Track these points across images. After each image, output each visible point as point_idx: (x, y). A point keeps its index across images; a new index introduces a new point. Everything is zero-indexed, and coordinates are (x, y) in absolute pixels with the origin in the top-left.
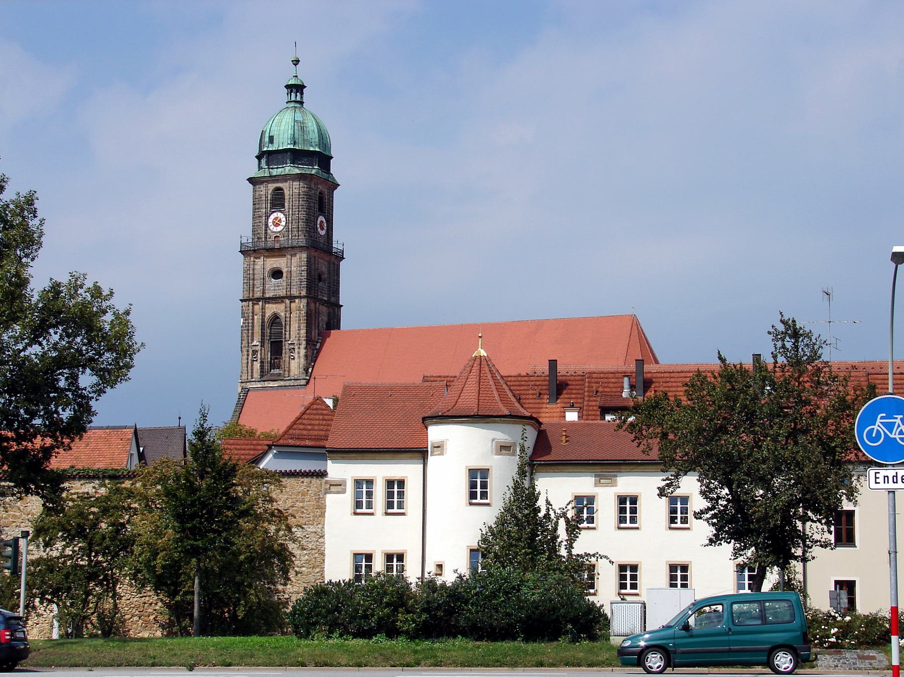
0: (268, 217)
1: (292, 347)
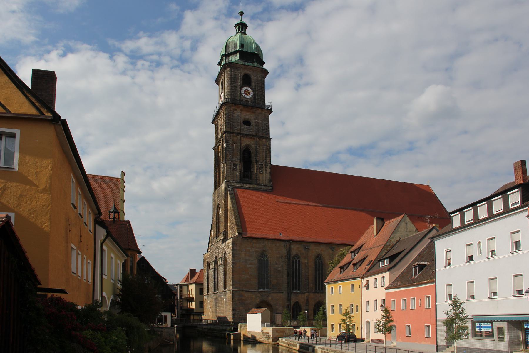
0: (241, 88)
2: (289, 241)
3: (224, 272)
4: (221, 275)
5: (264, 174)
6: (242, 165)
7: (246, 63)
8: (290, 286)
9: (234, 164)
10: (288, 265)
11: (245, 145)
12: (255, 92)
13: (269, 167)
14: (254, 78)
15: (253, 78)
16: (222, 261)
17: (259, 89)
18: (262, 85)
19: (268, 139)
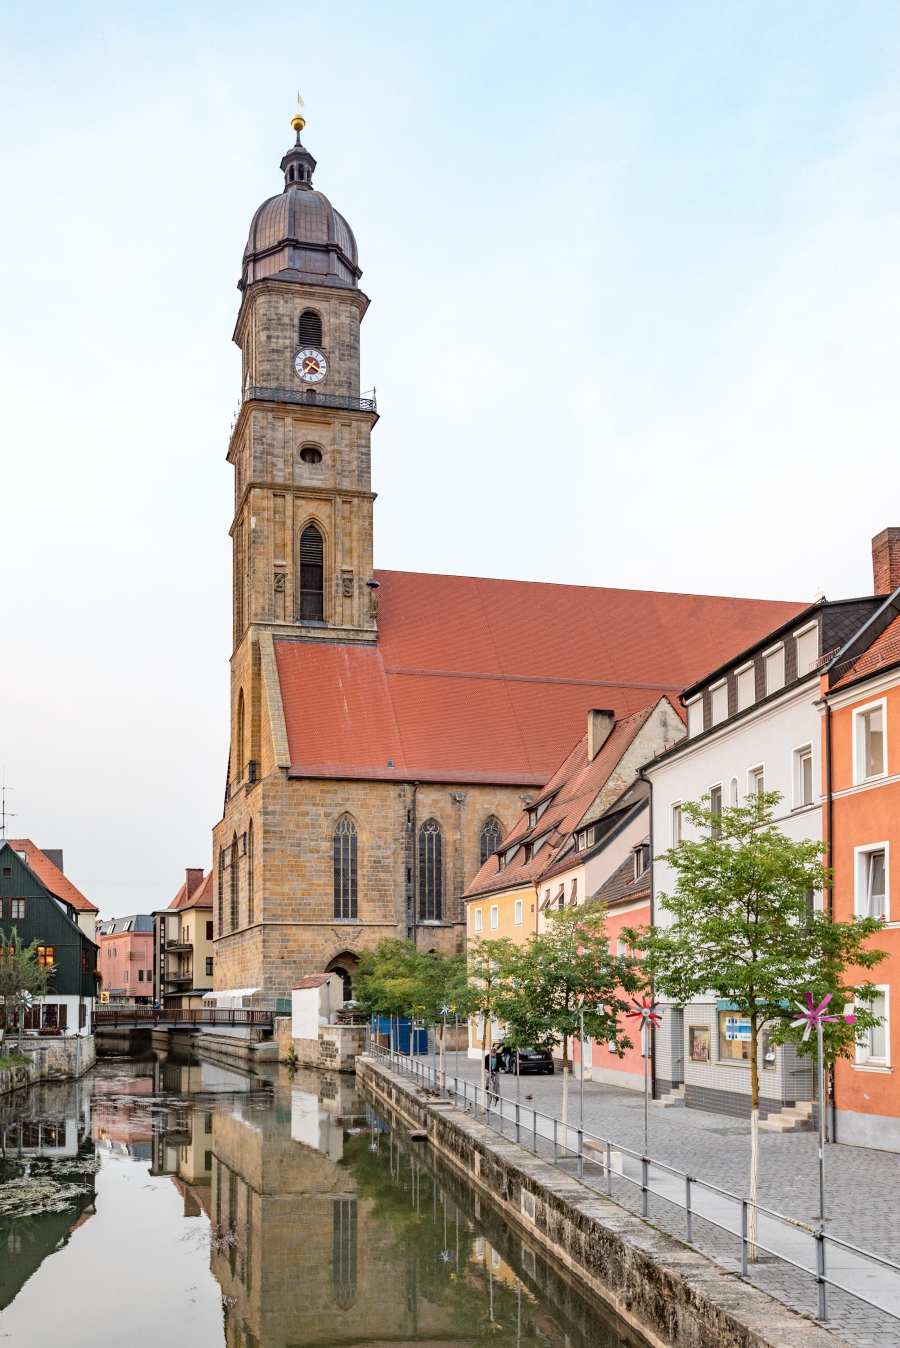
2: (411, 783)
3: (250, 873)
5: (356, 600)
8: (415, 907)
10: (407, 849)
15: (328, 322)
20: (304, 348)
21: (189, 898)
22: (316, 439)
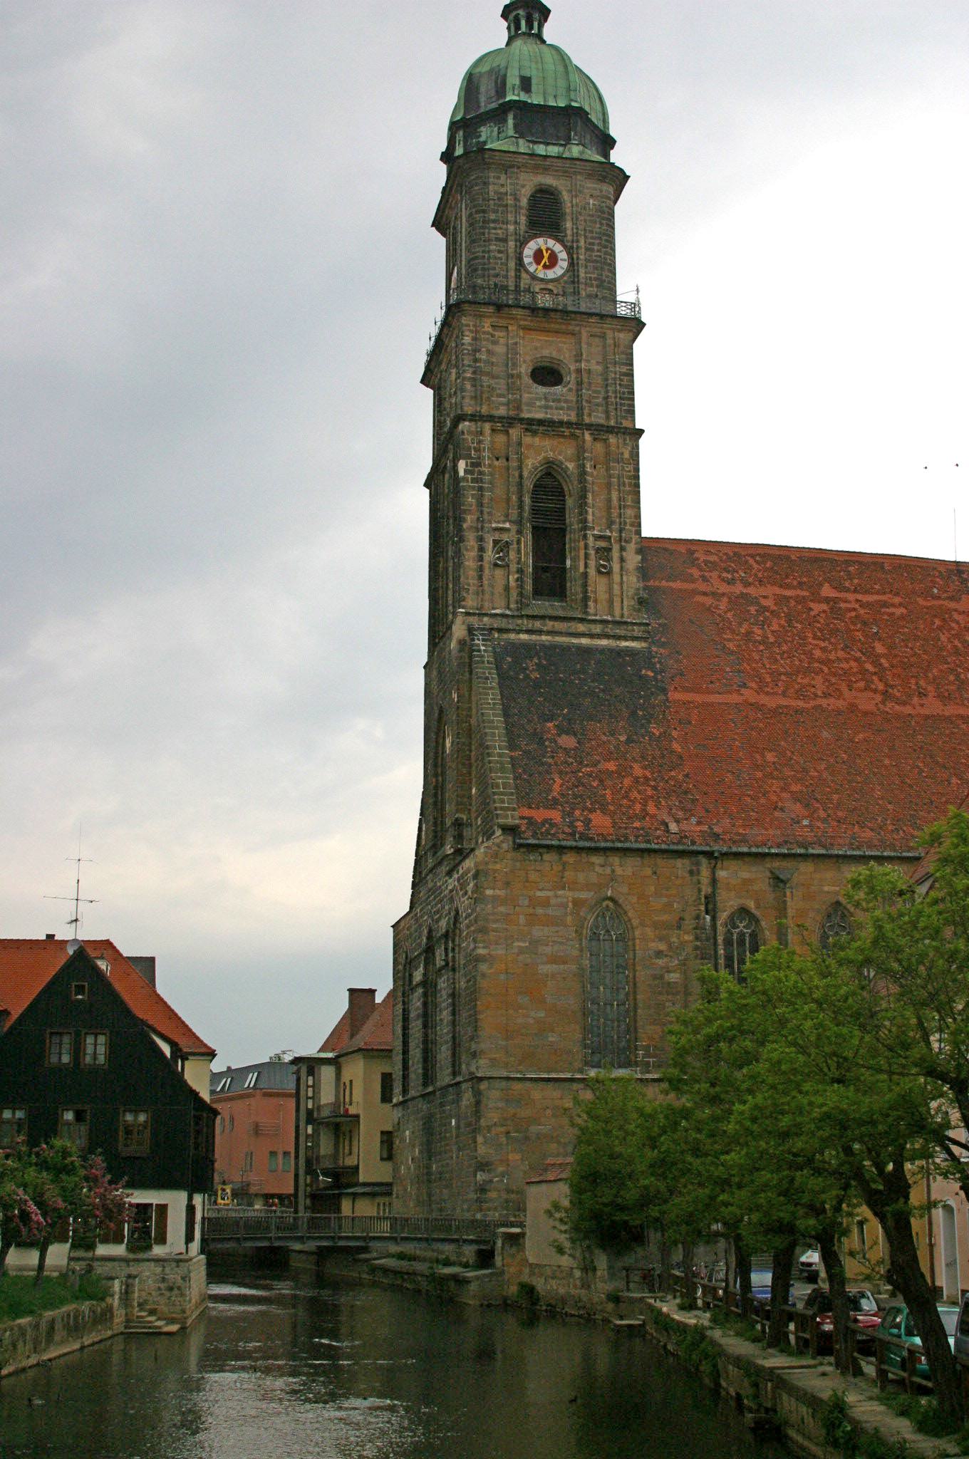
0: (522, 244)
1: (602, 544)
4: (445, 1013)
6: (530, 543)
7: (541, 149)
9: (496, 542)
11: (539, 462)
12: (575, 256)
13: (632, 547)
14: (572, 202)
16: (446, 949)
17: (592, 244)
18: (601, 224)
19: (630, 434)
20: (535, 236)
21: (352, 1036)
22: (554, 354)
